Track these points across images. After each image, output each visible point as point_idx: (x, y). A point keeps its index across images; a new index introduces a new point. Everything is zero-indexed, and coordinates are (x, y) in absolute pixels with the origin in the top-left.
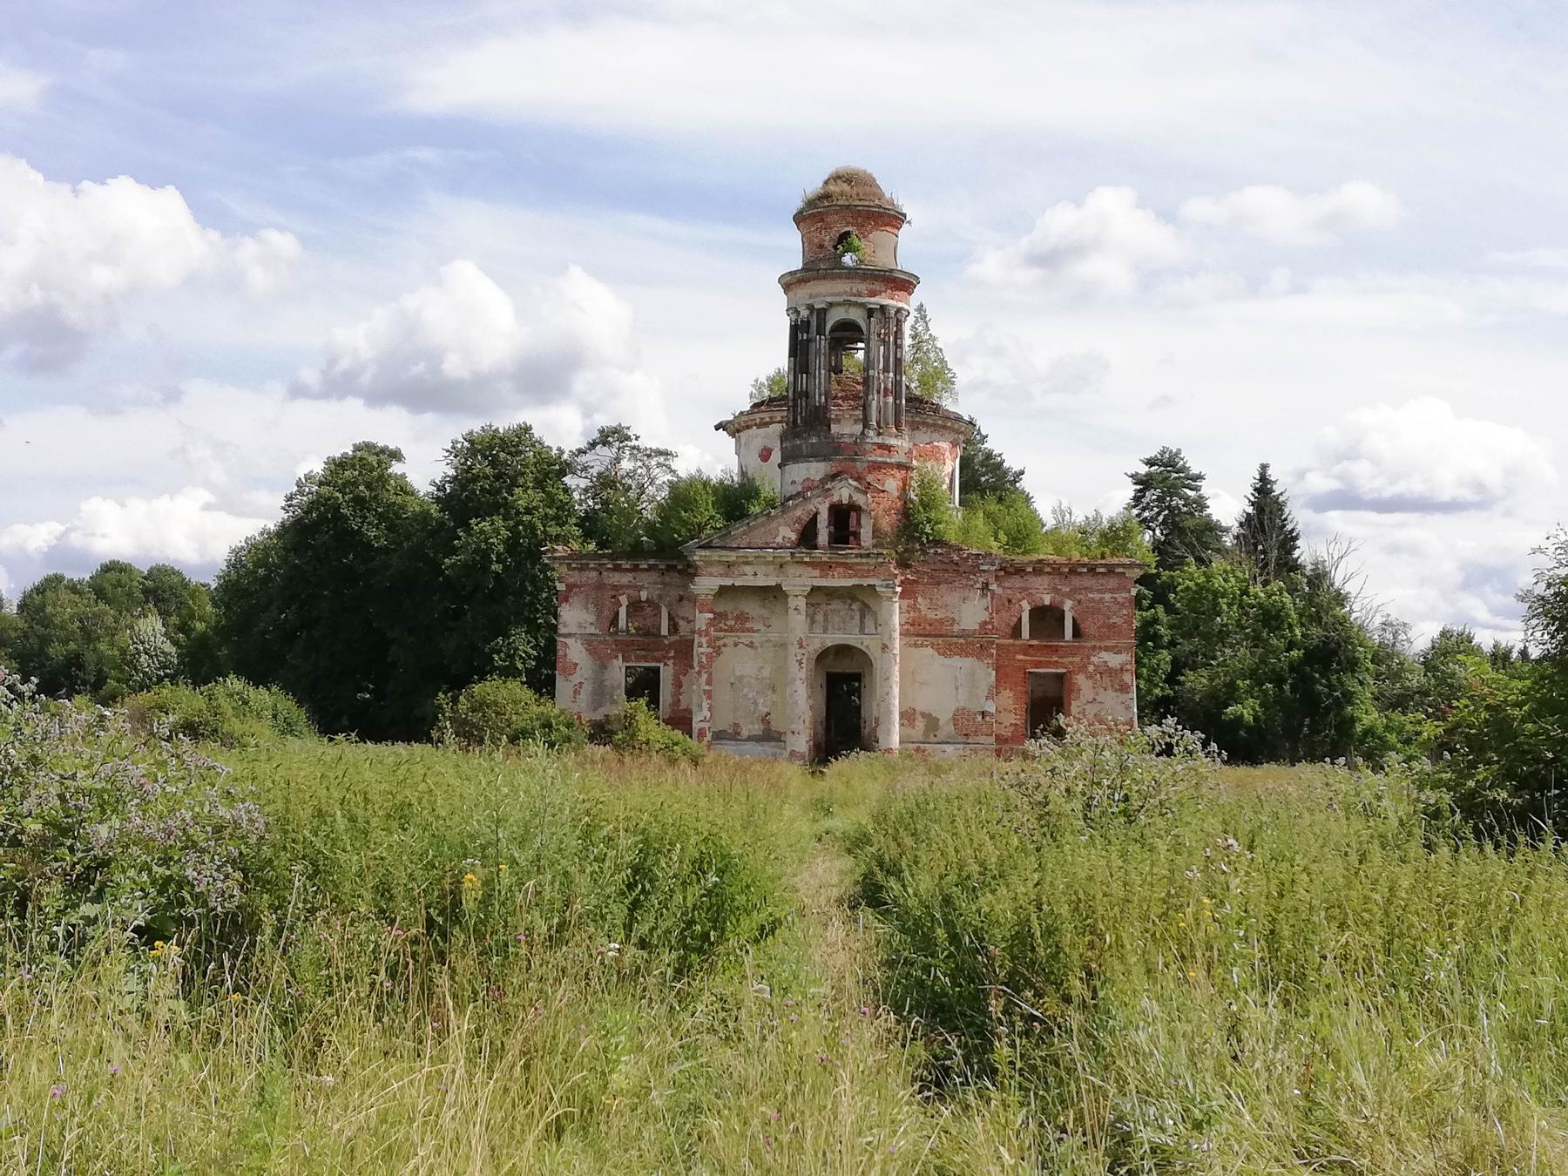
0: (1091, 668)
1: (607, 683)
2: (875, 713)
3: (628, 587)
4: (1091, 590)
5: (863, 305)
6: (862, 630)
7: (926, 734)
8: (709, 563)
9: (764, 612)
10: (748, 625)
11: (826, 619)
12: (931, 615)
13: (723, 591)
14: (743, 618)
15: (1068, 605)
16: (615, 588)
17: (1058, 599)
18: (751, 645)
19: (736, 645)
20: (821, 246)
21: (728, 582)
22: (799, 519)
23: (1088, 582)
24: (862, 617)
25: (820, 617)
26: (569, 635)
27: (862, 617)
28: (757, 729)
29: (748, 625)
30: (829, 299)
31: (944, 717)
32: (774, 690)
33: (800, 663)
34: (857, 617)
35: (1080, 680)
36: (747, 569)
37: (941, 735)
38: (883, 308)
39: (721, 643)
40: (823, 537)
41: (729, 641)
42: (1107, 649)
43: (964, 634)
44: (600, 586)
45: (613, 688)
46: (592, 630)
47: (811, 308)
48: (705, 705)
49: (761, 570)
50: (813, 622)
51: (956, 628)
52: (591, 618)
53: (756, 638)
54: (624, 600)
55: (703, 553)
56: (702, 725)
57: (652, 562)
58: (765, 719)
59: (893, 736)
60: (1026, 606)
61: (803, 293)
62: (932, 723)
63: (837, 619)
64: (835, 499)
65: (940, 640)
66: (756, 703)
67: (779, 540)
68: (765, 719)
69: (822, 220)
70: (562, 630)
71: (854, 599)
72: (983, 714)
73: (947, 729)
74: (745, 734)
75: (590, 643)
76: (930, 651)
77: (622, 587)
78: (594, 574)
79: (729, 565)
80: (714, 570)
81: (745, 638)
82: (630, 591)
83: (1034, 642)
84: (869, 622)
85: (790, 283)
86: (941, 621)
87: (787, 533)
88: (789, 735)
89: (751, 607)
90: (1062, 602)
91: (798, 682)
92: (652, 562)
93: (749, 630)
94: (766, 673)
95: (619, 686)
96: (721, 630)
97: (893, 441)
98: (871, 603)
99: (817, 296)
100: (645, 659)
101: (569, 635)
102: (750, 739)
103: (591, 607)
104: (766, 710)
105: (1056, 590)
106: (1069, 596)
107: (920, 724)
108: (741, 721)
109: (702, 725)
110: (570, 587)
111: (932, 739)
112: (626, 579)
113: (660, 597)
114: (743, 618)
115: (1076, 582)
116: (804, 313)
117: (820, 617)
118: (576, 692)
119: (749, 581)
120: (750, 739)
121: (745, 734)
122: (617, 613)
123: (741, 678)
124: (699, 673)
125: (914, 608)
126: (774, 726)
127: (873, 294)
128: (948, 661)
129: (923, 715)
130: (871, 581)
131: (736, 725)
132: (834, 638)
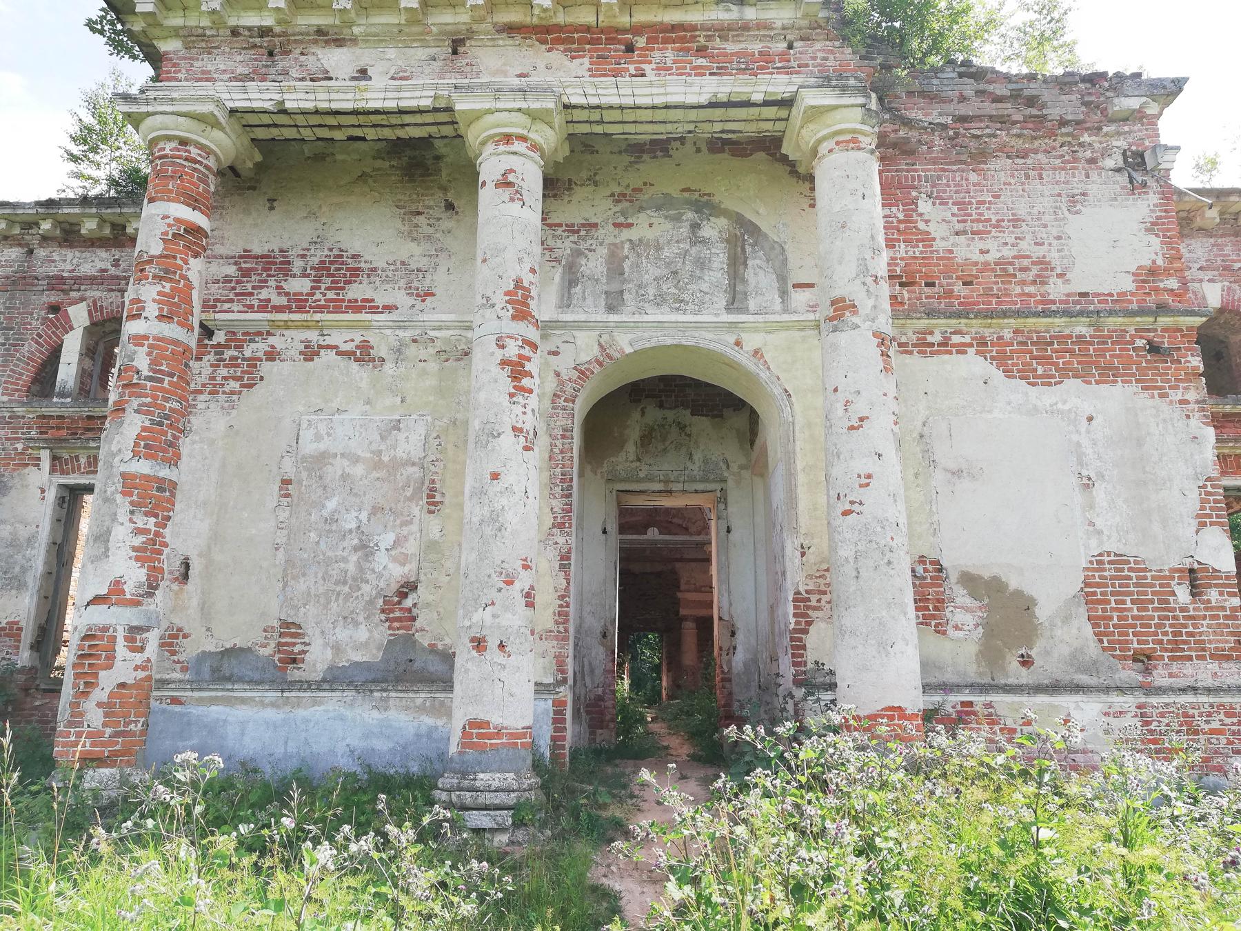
2: (796, 578)
3: (92, 280)
6: (736, 299)
7: (990, 654)
9: (412, 251)
11: (615, 268)
12: (968, 251)
14: (339, 271)
18: (363, 354)
19: (310, 353)
24: (737, 263)
25: (595, 265)
27: (737, 263)
28: (364, 640)
29: (355, 292)
31: (1053, 589)
32: (433, 502)
33: (517, 370)
34: (719, 258)
36: (337, 60)
37: (1049, 664)
39: (260, 347)
41: (289, 342)
43: (1082, 306)
48: (123, 537)
49: (384, 63)
50: (572, 279)
51: (1056, 290)
54: (79, 315)
56: (100, 616)
58: (399, 603)
59: (880, 660)
62: (1008, 614)
63: (651, 271)
65: (1006, 329)
66: (365, 549)
71: (705, 207)
72: (1195, 578)
73: (1067, 637)
74: (318, 658)
76: (973, 365)
77: (79, 281)
82: (95, 293)
84: (759, 277)
86: (1004, 270)
88: (465, 659)
89: (370, 232)
91: (508, 444)
93: (355, 306)
94: (410, 443)
95: (30, 541)
96: (265, 306)
98: (763, 216)
102: (337, 679)
104: (398, 573)
107: (964, 615)
108: (308, 616)
109: (100, 616)
111: (1016, 673)
114: (339, 271)
117: (595, 265)
120: (335, 679)
121: (318, 658)
122: (55, 354)
123: (322, 458)
124: (120, 409)
126: (430, 628)
128: (1044, 397)
129: (969, 580)
130: (780, 85)
131: (290, 629)
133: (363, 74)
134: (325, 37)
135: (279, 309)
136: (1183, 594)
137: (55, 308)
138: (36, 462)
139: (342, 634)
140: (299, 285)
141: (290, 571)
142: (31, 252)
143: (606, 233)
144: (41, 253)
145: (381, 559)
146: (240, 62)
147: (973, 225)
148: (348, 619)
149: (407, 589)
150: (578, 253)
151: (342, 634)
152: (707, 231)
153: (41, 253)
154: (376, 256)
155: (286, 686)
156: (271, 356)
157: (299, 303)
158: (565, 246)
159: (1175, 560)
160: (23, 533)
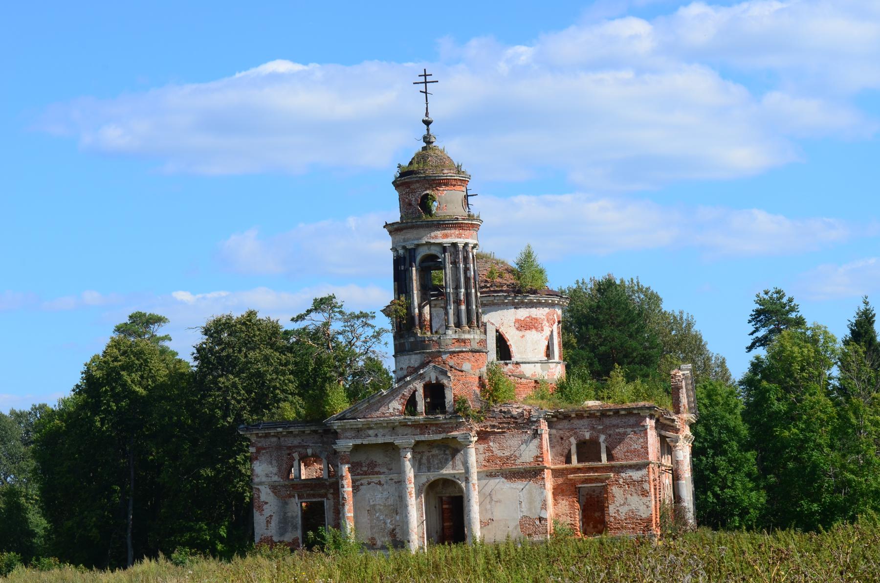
0: (621, 481)
1: (289, 514)
4: (618, 426)
5: (440, 244)
8: (344, 430)
10: (376, 469)
12: (500, 454)
13: (356, 448)
14: (373, 465)
15: (602, 438)
16: (289, 448)
17: (595, 434)
18: (380, 483)
19: (369, 484)
20: (410, 204)
21: (358, 442)
23: (615, 421)
25: (424, 461)
26: (261, 483)
29: (376, 469)
30: (416, 242)
35: (615, 490)
36: (371, 432)
38: (454, 245)
39: (358, 483)
40: (421, 406)
41: (365, 481)
42: (631, 467)
44: (279, 447)
45: (292, 517)
46: (276, 478)
47: (404, 248)
49: (381, 432)
52: (275, 470)
53: (382, 478)
57: (313, 428)
60: (573, 441)
61: (400, 237)
64: (427, 379)
66: (385, 523)
67: (391, 410)
68: (393, 533)
69: (409, 187)
70: (256, 480)
72: (540, 519)
75: (274, 488)
78: (274, 439)
79: (358, 430)
80: (348, 434)
81: (375, 479)
83: (580, 465)
85: (393, 229)
89: (379, 458)
90: (598, 437)
92: (313, 428)
95: (297, 516)
96: (358, 474)
97: (467, 336)
99: (408, 240)
100: (314, 496)
101: (261, 483)
103: (274, 462)
105: (593, 428)
106: (602, 432)
108: (376, 536)
110: (259, 450)
112: (296, 441)
113: (321, 452)
115: (607, 421)
116: (401, 252)
117: (424, 461)
118: (268, 522)
119: (373, 440)
121: (379, 543)
123: (374, 505)
125: (489, 450)
127: (446, 236)
131: (373, 539)
132: (433, 476)
133: (376, 435)
135: (362, 474)
136: (538, 522)
137: (289, 454)
138: (294, 496)
139: (383, 539)
140: (365, 469)
141: (372, 527)
143: (427, 454)
144: (282, 439)
145: (389, 525)
146: (353, 434)
147: (502, 448)
148: (383, 536)
149: (394, 530)
150: (421, 458)
151: (383, 539)
152: (447, 452)
153: (282, 439)
154: (379, 461)
155: (374, 549)
156: (362, 484)
157: (365, 473)
158: (419, 456)
159: (534, 516)
160: (294, 515)
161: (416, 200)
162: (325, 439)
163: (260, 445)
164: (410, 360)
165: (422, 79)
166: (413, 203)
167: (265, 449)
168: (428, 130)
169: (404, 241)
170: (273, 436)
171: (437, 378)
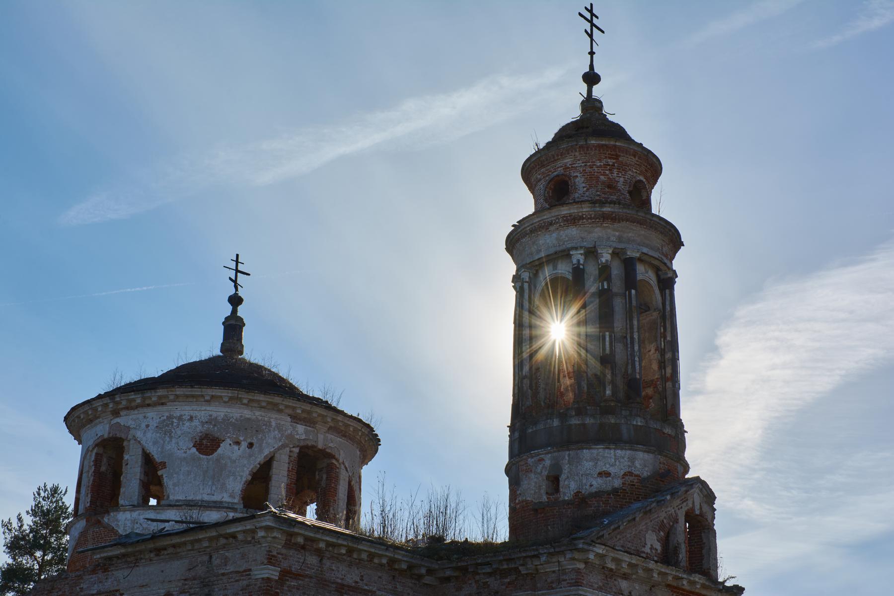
22: (662, 526)
30: (645, 250)
55: (600, 550)
67: (647, 549)
69: (617, 157)
78: (313, 560)
87: (652, 542)
134: (625, 577)
142: (321, 560)
153: (327, 563)
161: (625, 182)
162: (400, 588)
163: (285, 564)
164: (632, 460)
165: (588, 15)
166: (620, 185)
167: (297, 576)
168: (590, 92)
169: (620, 239)
170: (319, 553)
171: (701, 508)
